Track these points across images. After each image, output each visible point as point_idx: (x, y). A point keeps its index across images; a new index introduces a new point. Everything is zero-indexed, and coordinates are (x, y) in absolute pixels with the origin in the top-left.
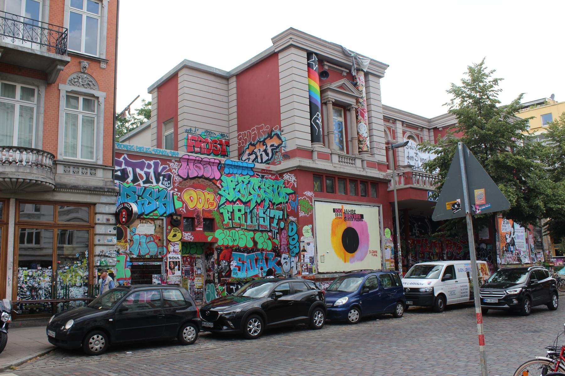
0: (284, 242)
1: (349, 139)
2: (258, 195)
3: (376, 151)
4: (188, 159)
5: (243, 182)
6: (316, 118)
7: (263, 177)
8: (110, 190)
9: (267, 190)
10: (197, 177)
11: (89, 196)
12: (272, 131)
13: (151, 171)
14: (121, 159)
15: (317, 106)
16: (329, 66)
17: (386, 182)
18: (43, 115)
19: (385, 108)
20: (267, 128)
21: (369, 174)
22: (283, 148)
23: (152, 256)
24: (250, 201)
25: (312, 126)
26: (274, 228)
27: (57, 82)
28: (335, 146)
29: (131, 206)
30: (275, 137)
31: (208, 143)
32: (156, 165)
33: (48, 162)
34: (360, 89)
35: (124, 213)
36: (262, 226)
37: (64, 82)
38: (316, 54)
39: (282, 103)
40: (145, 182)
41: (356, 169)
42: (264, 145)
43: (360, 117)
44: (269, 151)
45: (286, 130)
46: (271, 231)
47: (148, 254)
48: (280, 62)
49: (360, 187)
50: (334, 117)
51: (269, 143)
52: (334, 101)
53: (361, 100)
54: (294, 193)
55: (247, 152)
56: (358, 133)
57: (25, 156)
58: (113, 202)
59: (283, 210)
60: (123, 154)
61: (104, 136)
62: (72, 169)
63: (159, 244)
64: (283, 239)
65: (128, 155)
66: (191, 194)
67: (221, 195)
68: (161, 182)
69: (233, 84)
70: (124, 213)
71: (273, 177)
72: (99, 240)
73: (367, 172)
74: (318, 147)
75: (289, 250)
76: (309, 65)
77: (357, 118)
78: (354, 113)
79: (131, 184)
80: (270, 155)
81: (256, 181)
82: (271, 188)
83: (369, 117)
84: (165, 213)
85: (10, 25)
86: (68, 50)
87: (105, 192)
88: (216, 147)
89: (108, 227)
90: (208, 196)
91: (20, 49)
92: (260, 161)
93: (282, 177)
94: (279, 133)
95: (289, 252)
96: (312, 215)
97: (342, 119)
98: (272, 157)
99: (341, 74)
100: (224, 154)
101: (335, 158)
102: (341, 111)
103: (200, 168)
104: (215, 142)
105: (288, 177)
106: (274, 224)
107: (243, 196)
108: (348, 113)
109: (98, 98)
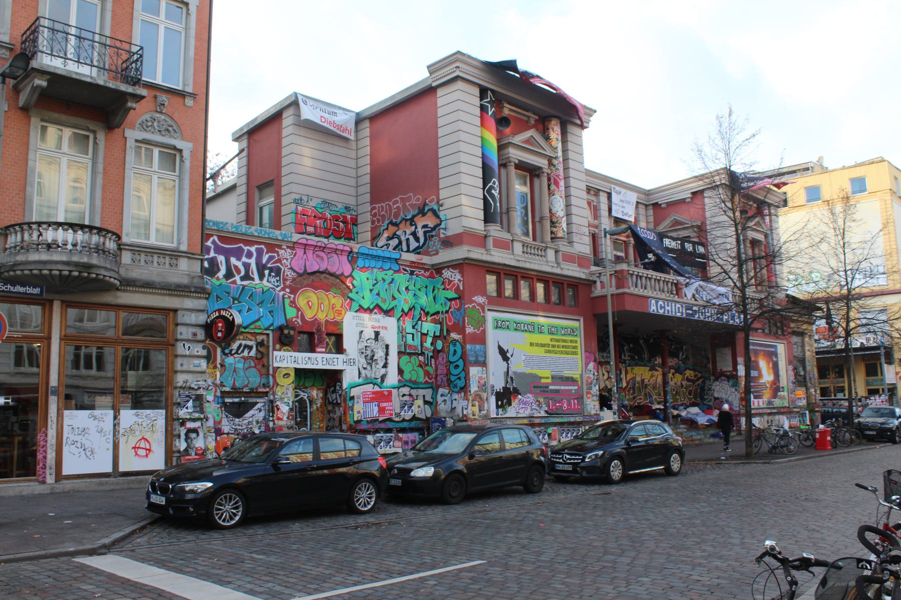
0: (442, 370)
1: (537, 219)
2: (405, 300)
3: (575, 238)
4: (306, 245)
5: (384, 280)
7: (412, 273)
9: (418, 293)
10: (318, 272)
11: (167, 298)
12: (425, 204)
13: (253, 261)
14: (209, 243)
15: (493, 170)
16: (511, 110)
17: (589, 284)
18: (101, 176)
19: (589, 173)
20: (418, 200)
21: (565, 273)
22: (442, 231)
23: (252, 389)
24: (393, 309)
25: (485, 199)
26: (427, 349)
27: (122, 127)
28: (518, 229)
30: (430, 214)
31: (326, 220)
32: (260, 253)
33: (111, 245)
34: (554, 144)
35: (220, 325)
36: (410, 346)
37: (132, 127)
38: (492, 91)
39: (442, 163)
40: (242, 279)
41: (547, 264)
42: (412, 225)
43: (553, 187)
44: (420, 234)
45: (447, 203)
46: (422, 354)
47: (246, 386)
48: (440, 102)
49: (554, 291)
51: (420, 222)
52: (517, 162)
53: (555, 162)
55: (386, 235)
57: (80, 236)
58: (202, 308)
59: (441, 323)
60: (212, 235)
61: (190, 209)
62: (143, 257)
63: (264, 371)
64: (440, 367)
65: (220, 237)
66: (309, 297)
67: (352, 300)
68: (266, 279)
71: (427, 274)
72: (182, 365)
73: (562, 269)
74: (495, 231)
75: (449, 383)
76: (483, 108)
77: (549, 189)
78: (545, 179)
79: (223, 281)
80: (422, 240)
81: (402, 279)
82: (424, 290)
83: (567, 187)
84: (272, 325)
85: (87, 47)
86: (143, 79)
87: (191, 292)
88: (338, 226)
90: (333, 301)
91: (74, 76)
92: (405, 248)
93: (441, 275)
94: (436, 207)
95: (449, 385)
96: (484, 332)
97: (526, 189)
98: (424, 244)
99: (527, 122)
100: (349, 237)
101: (518, 247)
102: (525, 177)
103: (322, 259)
104: (336, 218)
106: (428, 344)
107: (384, 301)
109: (180, 151)
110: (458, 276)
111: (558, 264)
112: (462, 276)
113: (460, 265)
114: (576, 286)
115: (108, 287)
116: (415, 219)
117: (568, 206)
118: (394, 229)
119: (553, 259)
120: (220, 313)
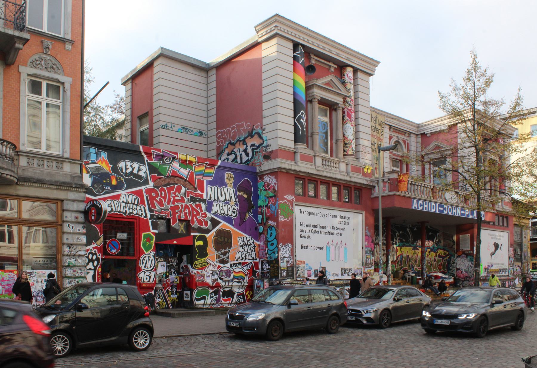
1: (334, 141)
3: (361, 155)
6: (300, 117)
8: (78, 186)
11: (55, 192)
12: (253, 129)
17: (370, 188)
20: (248, 126)
21: (353, 180)
29: (100, 204)
30: (256, 136)
35: (93, 211)
42: (244, 144)
43: (346, 118)
44: (250, 151)
45: (268, 128)
49: (345, 192)
50: (319, 117)
51: (250, 142)
54: (275, 196)
55: (226, 152)
56: (344, 135)
58: (81, 199)
62: (36, 161)
69: (213, 77)
70: (93, 211)
73: (350, 177)
74: (302, 148)
77: (343, 119)
78: (340, 112)
80: (250, 155)
83: (356, 118)
87: (73, 187)
89: (77, 225)
92: (239, 161)
94: (260, 131)
96: (292, 221)
97: (327, 120)
101: (319, 161)
102: (326, 110)
105: (269, 179)
108: (334, 113)
110: (274, 181)
111: (348, 173)
112: (277, 181)
113: (275, 173)
114: (361, 189)
115: (9, 183)
116: (246, 140)
117: (356, 132)
118: (233, 147)
119: (345, 170)
120: (93, 203)
